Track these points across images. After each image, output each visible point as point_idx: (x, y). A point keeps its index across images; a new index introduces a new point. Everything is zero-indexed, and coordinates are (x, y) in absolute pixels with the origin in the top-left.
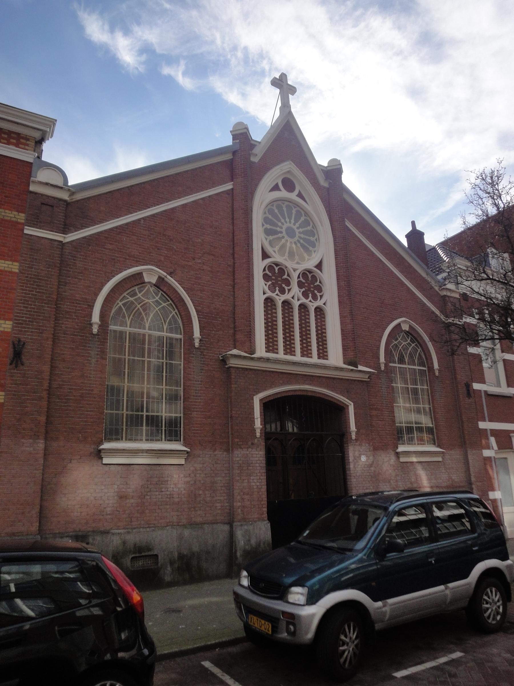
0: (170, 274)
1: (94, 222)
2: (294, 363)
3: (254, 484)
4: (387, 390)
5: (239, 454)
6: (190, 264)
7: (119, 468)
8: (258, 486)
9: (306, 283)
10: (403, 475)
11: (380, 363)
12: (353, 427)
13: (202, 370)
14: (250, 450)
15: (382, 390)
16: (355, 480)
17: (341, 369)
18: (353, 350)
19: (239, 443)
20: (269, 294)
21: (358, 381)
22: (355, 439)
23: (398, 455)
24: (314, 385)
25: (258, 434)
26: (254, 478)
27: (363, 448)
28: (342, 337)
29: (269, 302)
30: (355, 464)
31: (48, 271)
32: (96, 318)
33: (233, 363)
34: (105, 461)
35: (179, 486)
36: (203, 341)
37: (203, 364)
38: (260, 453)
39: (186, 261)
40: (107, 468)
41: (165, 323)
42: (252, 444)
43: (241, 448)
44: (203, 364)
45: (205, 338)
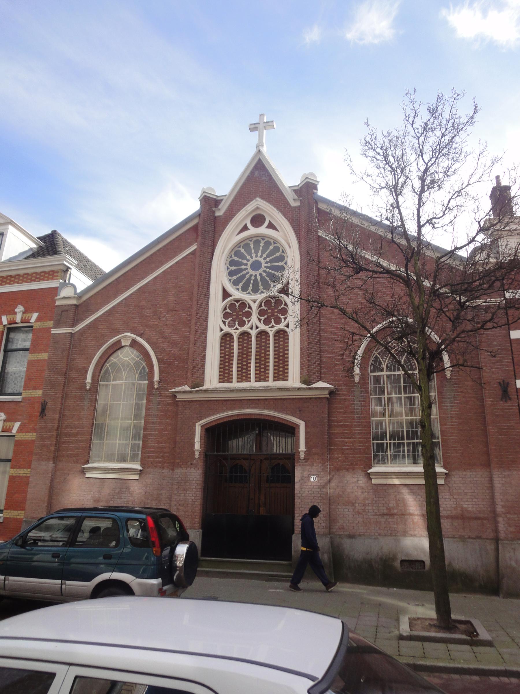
0: (141, 336)
1: (93, 312)
2: (232, 391)
3: (189, 498)
4: (361, 404)
5: (179, 472)
6: (156, 323)
7: (98, 480)
8: (192, 499)
10: (376, 499)
12: (302, 447)
13: (159, 406)
14: (189, 469)
15: (354, 404)
16: (299, 501)
17: (299, 389)
18: (307, 368)
19: (180, 463)
20: (226, 329)
21: (315, 398)
22: (304, 459)
23: (369, 476)
24: (260, 408)
25: (197, 456)
26: (190, 492)
27: (314, 467)
28: (301, 355)
29: (226, 338)
30: (302, 484)
31: (62, 354)
32: (89, 379)
33: (180, 397)
34: (87, 475)
35: (134, 496)
36: (162, 382)
37: (160, 401)
38: (198, 471)
39: (153, 322)
40: (88, 480)
41: (137, 373)
42: (191, 464)
43: (180, 467)
44: (160, 401)
45: (163, 380)
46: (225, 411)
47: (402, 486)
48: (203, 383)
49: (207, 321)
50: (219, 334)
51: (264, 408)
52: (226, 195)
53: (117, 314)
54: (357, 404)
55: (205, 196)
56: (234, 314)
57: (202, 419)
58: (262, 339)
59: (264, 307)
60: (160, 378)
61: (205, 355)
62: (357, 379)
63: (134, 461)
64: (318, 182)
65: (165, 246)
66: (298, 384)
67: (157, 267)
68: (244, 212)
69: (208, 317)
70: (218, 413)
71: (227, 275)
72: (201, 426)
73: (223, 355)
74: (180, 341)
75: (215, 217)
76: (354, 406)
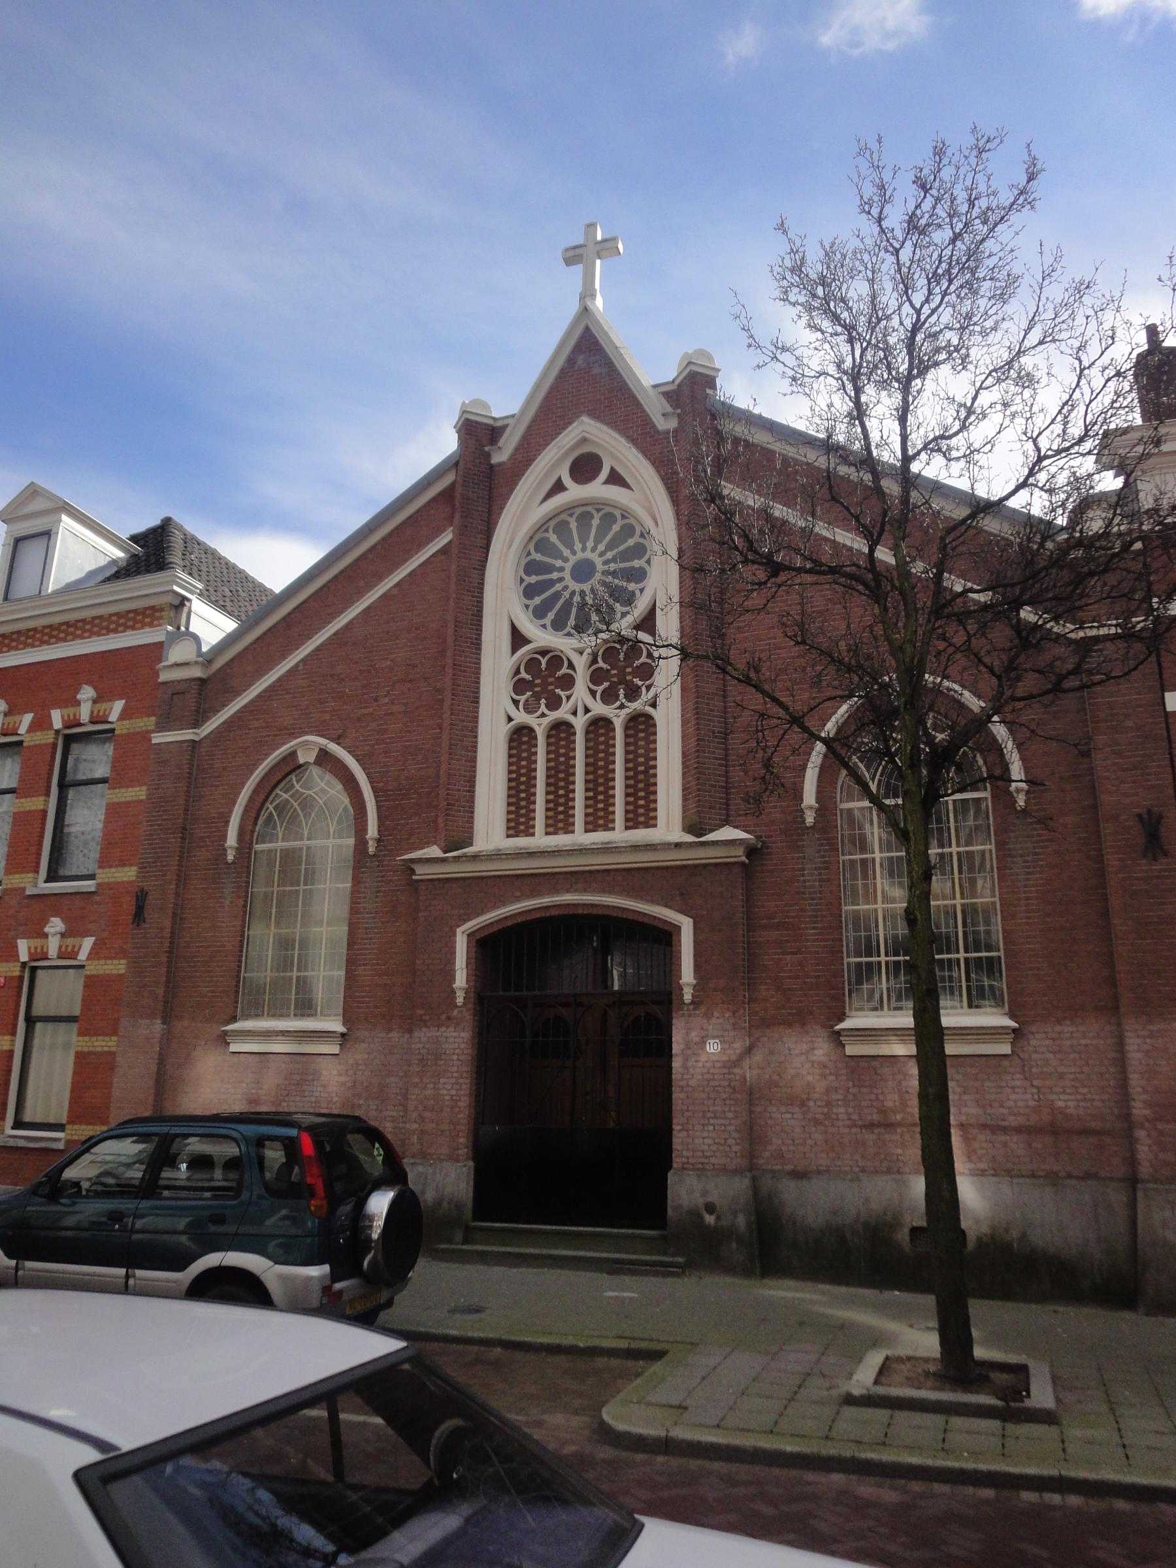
0: (337, 740)
1: (237, 693)
2: (532, 854)
3: (445, 1092)
4: (820, 874)
5: (422, 1035)
6: (370, 710)
7: (257, 1058)
8: (452, 1096)
9: (613, 668)
10: (855, 1090)
11: (802, 811)
12: (687, 974)
13: (379, 892)
14: (443, 1029)
15: (803, 875)
16: (682, 1095)
17: (678, 845)
19: (424, 1018)
20: (521, 717)
21: (716, 865)
22: (693, 1002)
23: (837, 1038)
24: (594, 891)
25: (460, 1000)
26: (446, 1080)
27: (714, 1020)
28: (683, 769)
29: (521, 737)
30: (686, 1059)
31: (176, 787)
32: (232, 840)
33: (422, 872)
34: (233, 1048)
35: (330, 1089)
36: (383, 841)
37: (382, 881)
38: (463, 1034)
40: (235, 1058)
42: (449, 1018)
43: (426, 1026)
44: (382, 881)
46: (518, 899)
47: (906, 1058)
48: (471, 838)
49: (476, 700)
50: (504, 729)
51: (603, 891)
52: (513, 416)
53: (288, 693)
54: (812, 875)
55: (467, 420)
56: (538, 681)
57: (469, 919)
58: (598, 735)
59: (601, 664)
60: (379, 831)
61: (474, 777)
62: (810, 819)
63: (303, 1015)
64: (718, 370)
65: (384, 539)
66: (677, 834)
67: (370, 587)
68: (555, 450)
69: (478, 693)
70: (504, 904)
71: (519, 596)
72: (469, 935)
73: (514, 776)
74: (422, 749)
75: (492, 467)
76: (805, 881)
